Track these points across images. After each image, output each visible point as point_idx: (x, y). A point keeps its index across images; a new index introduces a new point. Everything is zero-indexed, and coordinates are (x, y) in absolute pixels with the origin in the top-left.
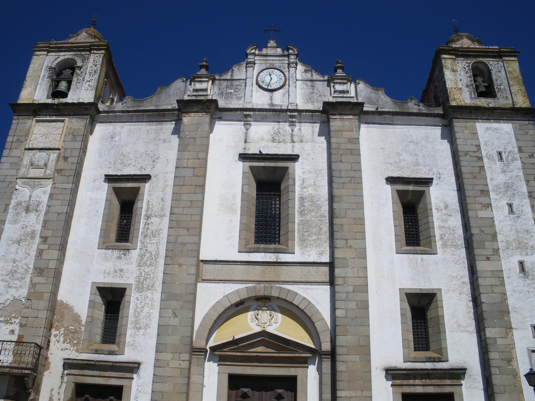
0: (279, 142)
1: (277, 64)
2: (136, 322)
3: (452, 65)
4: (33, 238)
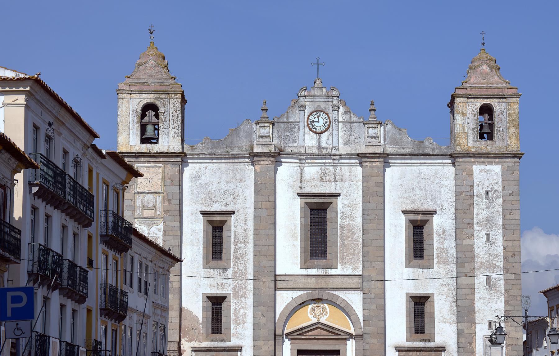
0: (325, 182)
1: (323, 107)
2: (236, 320)
3: (463, 109)
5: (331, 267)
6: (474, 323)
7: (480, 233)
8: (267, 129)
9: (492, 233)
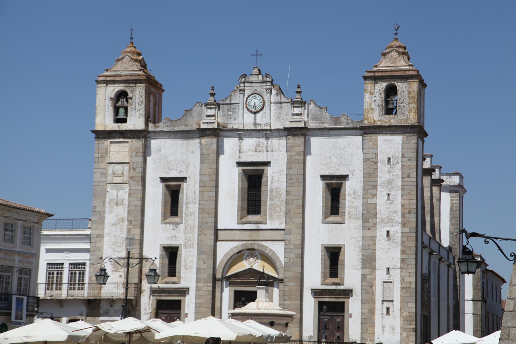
1: (259, 91)
2: (185, 266)
4: (123, 221)
5: (261, 223)
6: (374, 269)
7: (382, 193)
8: (213, 110)
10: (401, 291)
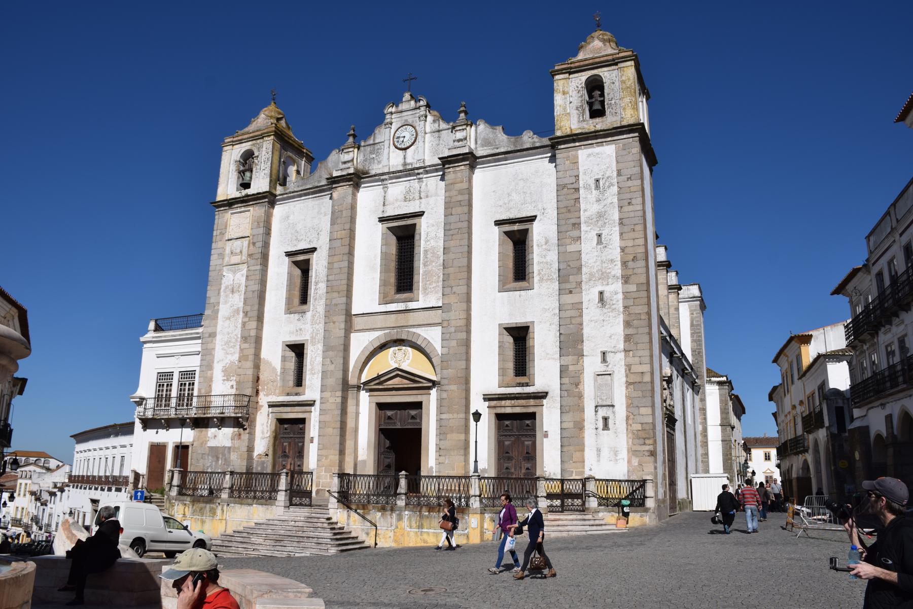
1: (410, 121)
2: (312, 369)
4: (238, 314)
7: (588, 234)
8: (351, 155)
9: (604, 233)
10: (627, 388)
